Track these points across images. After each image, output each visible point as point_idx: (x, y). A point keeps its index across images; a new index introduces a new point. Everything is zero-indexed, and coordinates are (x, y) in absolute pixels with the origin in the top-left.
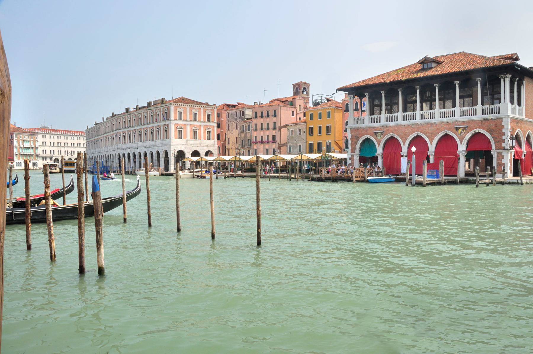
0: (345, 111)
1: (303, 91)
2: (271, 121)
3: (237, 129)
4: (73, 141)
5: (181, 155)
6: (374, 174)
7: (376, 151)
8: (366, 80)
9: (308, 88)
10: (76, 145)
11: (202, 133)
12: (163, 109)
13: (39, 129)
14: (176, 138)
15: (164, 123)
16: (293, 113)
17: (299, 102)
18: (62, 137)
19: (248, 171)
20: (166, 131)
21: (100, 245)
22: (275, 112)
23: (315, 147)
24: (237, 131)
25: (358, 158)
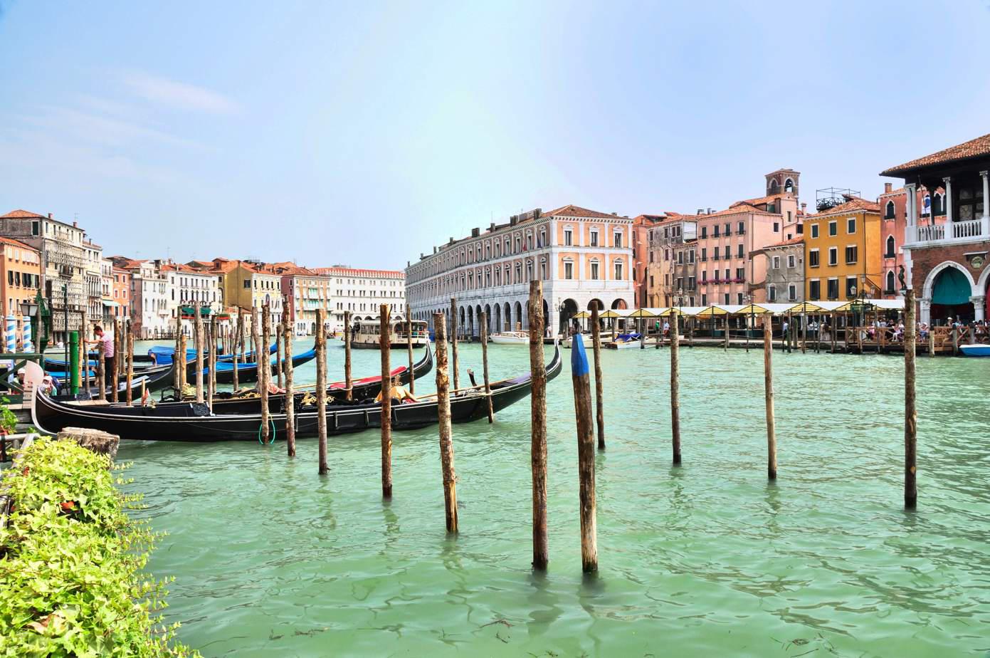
0: (886, 218)
1: (786, 187)
2: (734, 242)
3: (667, 259)
4: (383, 288)
5: (569, 308)
6: (973, 338)
7: (970, 294)
8: (943, 153)
9: (796, 180)
10: (388, 294)
11: (607, 268)
12: (538, 227)
13: (331, 269)
14: (561, 278)
15: (541, 252)
16: (776, 226)
17: (787, 205)
18: (367, 281)
19: (701, 334)
20: (544, 266)
21: (590, 507)
22: (742, 225)
23: (824, 289)
24: (668, 263)
25: (928, 308)
